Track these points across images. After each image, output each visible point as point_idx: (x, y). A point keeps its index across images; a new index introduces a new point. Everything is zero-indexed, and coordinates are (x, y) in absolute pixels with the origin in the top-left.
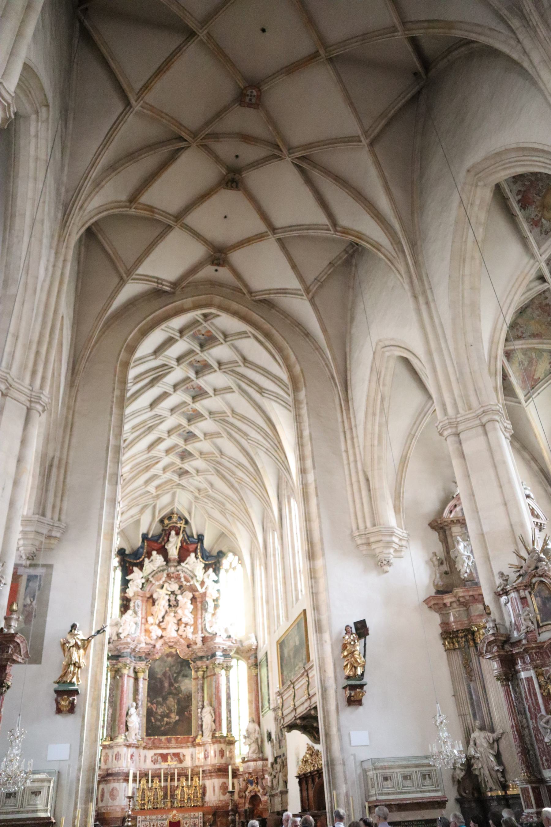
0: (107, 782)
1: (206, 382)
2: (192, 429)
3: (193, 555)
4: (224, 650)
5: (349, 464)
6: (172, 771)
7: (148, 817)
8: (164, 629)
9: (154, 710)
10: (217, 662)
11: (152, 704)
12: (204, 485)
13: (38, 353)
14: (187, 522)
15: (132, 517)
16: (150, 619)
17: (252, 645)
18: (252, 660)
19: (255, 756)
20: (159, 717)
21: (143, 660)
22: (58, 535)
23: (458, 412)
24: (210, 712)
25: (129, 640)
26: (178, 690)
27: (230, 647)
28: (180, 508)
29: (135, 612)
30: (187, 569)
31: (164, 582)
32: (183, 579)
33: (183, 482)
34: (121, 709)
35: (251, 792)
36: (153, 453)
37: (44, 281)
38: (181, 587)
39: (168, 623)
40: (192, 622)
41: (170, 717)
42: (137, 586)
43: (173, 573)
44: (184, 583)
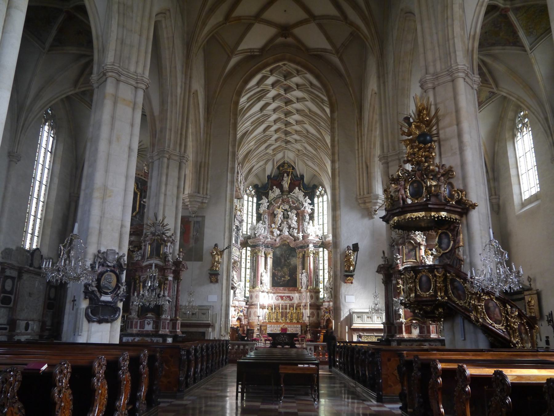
0: (252, 308)
1: (291, 95)
2: (288, 119)
3: (297, 188)
4: (314, 243)
5: (359, 157)
8: (281, 231)
10: (310, 249)
11: (275, 270)
12: (300, 148)
13: (181, 134)
14: (293, 168)
16: (273, 225)
19: (329, 300)
22: (206, 201)
23: (389, 151)
25: (261, 237)
26: (290, 264)
28: (289, 160)
29: (265, 222)
31: (281, 204)
33: (289, 146)
34: (258, 273)
36: (267, 133)
37: (181, 94)
38: (290, 207)
44: (292, 205)
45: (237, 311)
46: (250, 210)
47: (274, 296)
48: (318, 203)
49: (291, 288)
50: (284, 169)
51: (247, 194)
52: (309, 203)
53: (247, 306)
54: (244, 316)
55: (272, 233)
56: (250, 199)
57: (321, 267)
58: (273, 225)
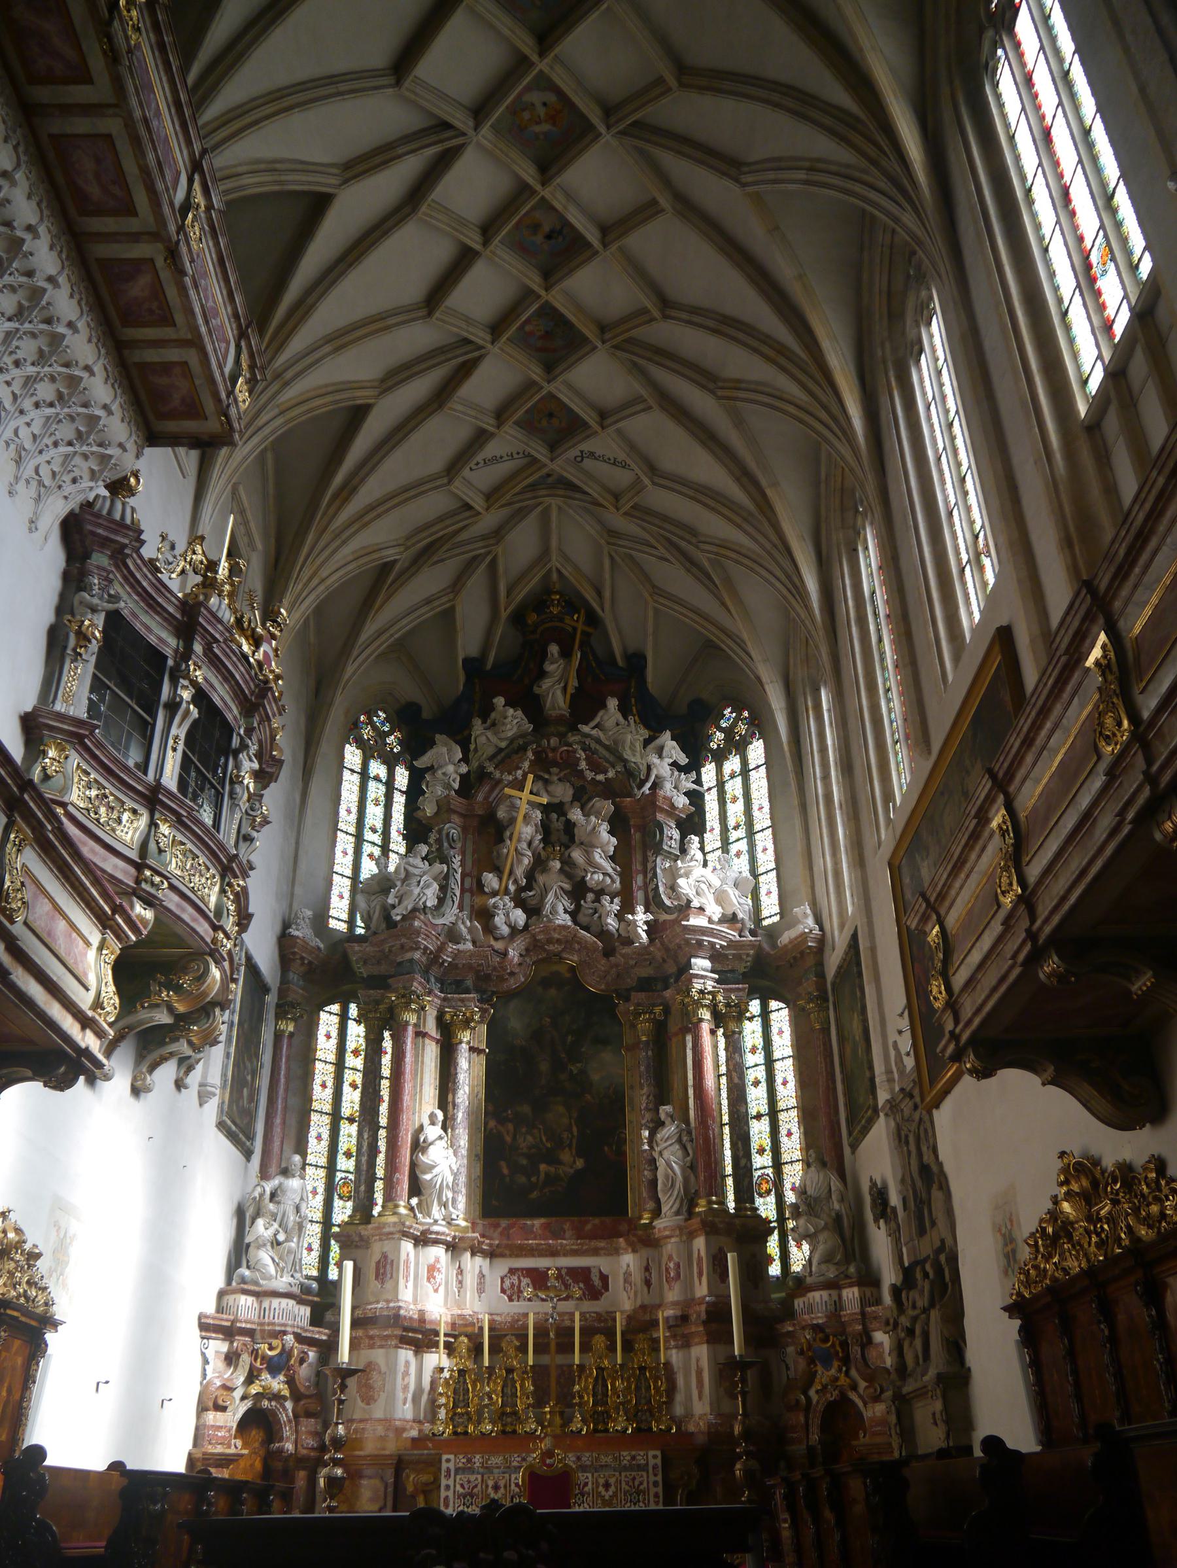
3: (613, 703)
6: (567, 1323)
7: (477, 1459)
8: (533, 911)
9: (508, 1139)
10: (697, 985)
11: (501, 1121)
14: (593, 619)
15: (428, 601)
16: (491, 880)
17: (804, 936)
18: (809, 985)
20: (524, 1162)
21: (468, 991)
24: (679, 1141)
27: (732, 944)
30: (598, 741)
32: (583, 765)
35: (825, 1387)
39: (546, 891)
40: (617, 885)
41: (559, 1162)
42: (448, 786)
43: (554, 750)
44: (589, 775)
45: (246, 1359)
46: (374, 815)
47: (495, 1272)
48: (721, 785)
49: (593, 1223)
50: (550, 619)
51: (360, 743)
52: (675, 764)
53: (322, 1334)
54: (296, 1396)
55: (485, 916)
56: (377, 768)
57: (757, 1098)
58: (491, 880)
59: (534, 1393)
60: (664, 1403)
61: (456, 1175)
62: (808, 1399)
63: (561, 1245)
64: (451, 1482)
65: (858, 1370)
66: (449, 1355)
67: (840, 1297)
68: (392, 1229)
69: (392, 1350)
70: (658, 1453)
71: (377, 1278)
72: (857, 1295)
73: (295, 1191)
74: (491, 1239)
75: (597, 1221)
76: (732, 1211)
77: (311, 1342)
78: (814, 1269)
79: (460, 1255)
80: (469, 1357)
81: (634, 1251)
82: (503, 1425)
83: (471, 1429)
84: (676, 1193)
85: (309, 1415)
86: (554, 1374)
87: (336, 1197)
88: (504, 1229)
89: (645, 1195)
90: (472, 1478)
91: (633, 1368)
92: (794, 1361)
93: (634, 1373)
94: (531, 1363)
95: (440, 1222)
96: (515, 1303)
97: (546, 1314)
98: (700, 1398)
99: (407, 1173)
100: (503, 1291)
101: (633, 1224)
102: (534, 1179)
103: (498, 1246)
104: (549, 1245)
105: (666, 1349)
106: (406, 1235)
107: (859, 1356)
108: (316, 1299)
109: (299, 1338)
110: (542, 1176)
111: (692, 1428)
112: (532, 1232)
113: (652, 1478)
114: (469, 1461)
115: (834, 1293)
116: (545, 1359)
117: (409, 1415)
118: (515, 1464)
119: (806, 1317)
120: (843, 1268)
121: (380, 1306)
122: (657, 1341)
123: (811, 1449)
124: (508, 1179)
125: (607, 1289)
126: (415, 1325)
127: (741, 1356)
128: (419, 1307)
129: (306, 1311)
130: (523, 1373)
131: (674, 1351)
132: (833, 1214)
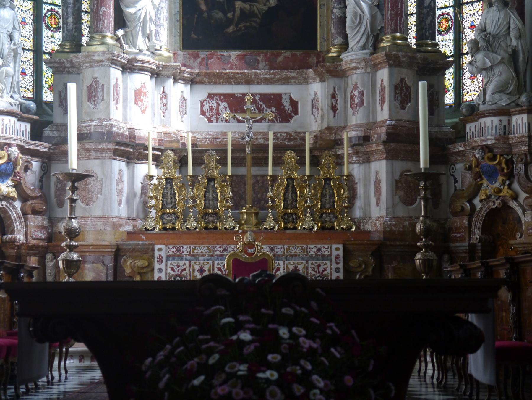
6: (261, 141)
7: (185, 249)
35: (488, 197)
53: (42, 147)
54: (24, 197)
59: (232, 198)
60: (346, 207)
61: (157, 9)
62: (473, 207)
63: (256, 74)
64: (163, 266)
65: (520, 184)
66: (157, 166)
67: (509, 122)
68: (101, 58)
69: (108, 162)
70: (341, 246)
71: (89, 99)
72: (525, 121)
73: (7, 21)
74: (191, 68)
75: (288, 54)
76: (415, 47)
77: (34, 153)
78: (487, 98)
79: (164, 82)
80: (175, 167)
81: (322, 80)
82: (205, 223)
83: (178, 225)
84: (363, 29)
85: (35, 212)
86: (249, 182)
87: (44, 28)
88: (203, 59)
89: (333, 31)
90: (181, 263)
91: (319, 179)
92: (461, 175)
93: (320, 184)
94: (229, 173)
95: (145, 52)
96: (214, 123)
97: (243, 133)
98: (378, 204)
99: (112, 7)
100: (203, 113)
101: (322, 58)
102: (230, 15)
103: (198, 74)
104: (245, 74)
105: (349, 163)
106: (114, 62)
107: (522, 172)
108: (35, 117)
109: (22, 149)
110: (238, 12)
111: (369, 227)
112: (229, 62)
113: (334, 266)
114: (178, 250)
115: (505, 119)
116: (242, 171)
117: (124, 214)
118: (218, 253)
119: (477, 139)
120: (515, 98)
121: (93, 124)
122: (341, 157)
123: (472, 246)
124: (205, 15)
125: (296, 113)
126: (126, 140)
127: (425, 169)
128: (129, 126)
129: (26, 127)
130: (223, 181)
131: (356, 166)
132: (510, 50)
